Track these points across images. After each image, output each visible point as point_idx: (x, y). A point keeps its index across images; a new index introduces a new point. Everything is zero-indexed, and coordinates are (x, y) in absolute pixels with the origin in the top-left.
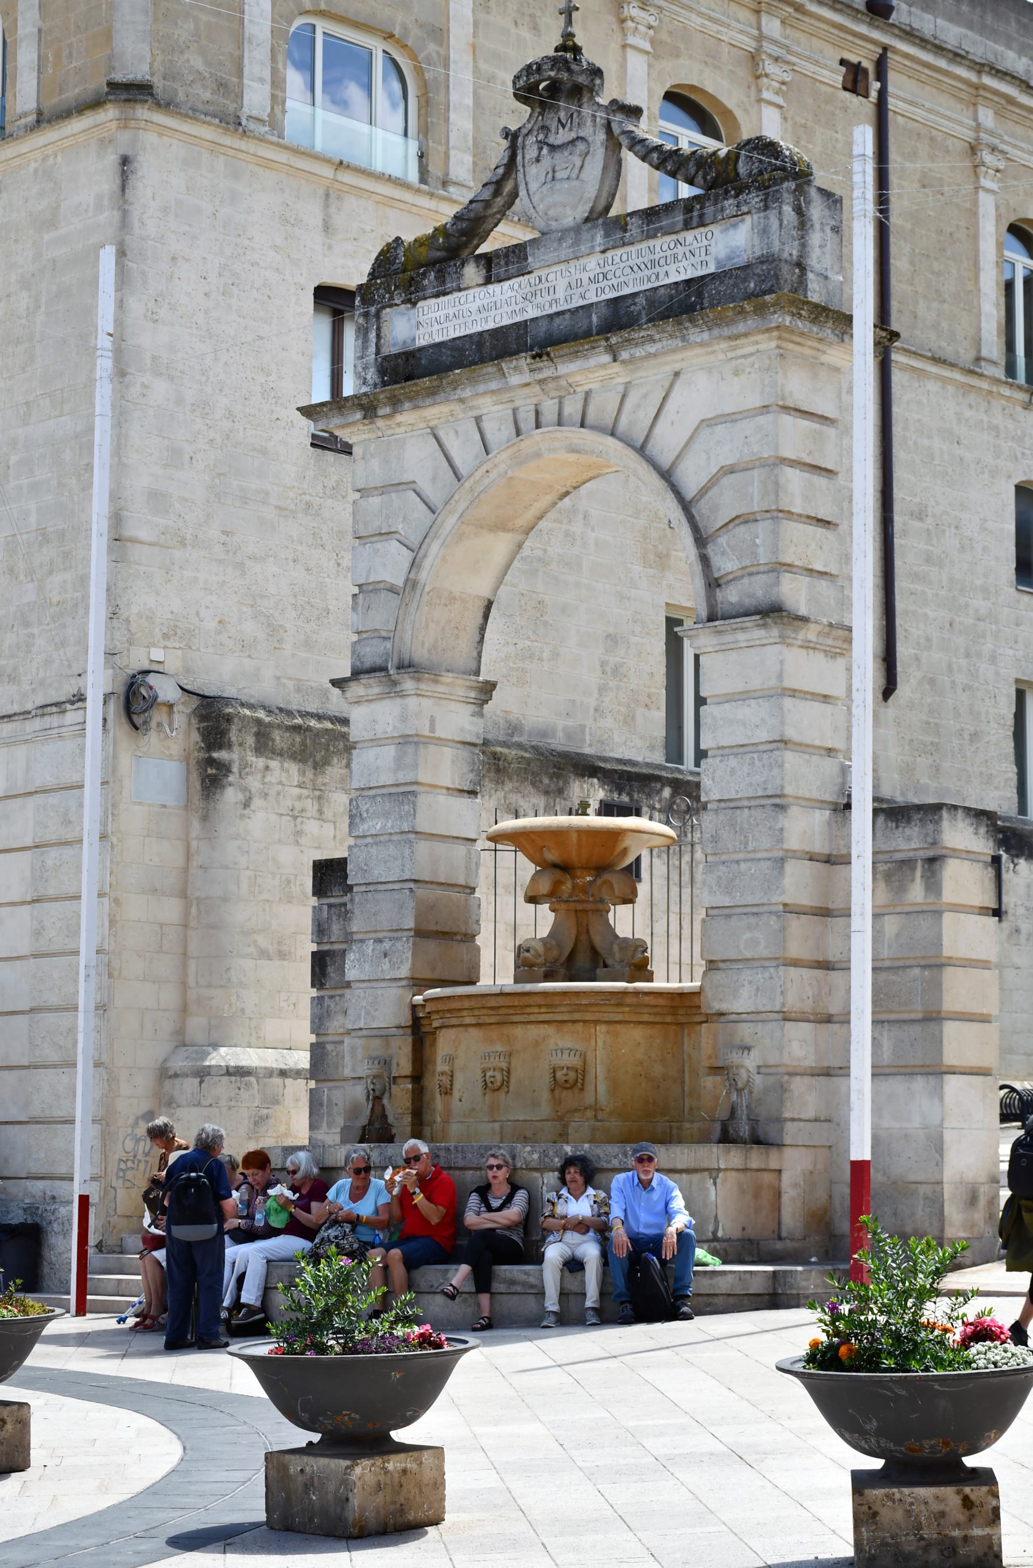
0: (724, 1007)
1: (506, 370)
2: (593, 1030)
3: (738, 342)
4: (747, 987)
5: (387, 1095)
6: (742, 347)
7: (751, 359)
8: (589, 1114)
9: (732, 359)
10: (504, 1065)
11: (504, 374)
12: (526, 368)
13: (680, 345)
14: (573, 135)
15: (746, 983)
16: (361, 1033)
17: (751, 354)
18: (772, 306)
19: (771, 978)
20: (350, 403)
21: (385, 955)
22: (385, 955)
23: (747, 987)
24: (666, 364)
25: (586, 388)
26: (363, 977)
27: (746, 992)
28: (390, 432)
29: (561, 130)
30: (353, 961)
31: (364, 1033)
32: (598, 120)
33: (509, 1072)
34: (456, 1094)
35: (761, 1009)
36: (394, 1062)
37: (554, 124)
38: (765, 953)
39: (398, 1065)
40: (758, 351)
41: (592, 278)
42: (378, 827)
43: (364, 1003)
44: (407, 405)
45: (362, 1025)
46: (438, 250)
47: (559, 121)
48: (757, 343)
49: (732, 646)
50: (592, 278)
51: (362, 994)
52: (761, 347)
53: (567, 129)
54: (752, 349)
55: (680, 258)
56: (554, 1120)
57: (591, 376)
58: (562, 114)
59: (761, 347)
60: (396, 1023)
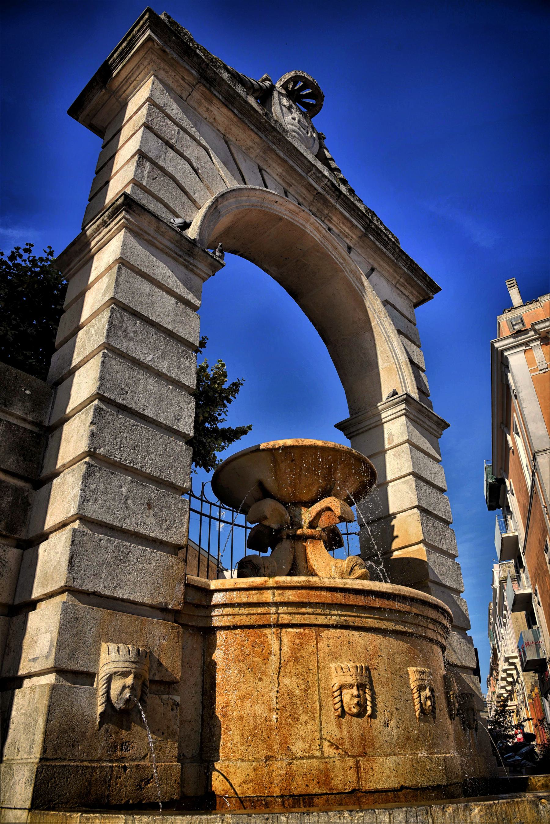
1: (312, 172)
3: (408, 286)
6: (406, 288)
9: (398, 288)
17: (405, 295)
20: (199, 61)
21: (149, 505)
22: (149, 505)
24: (375, 260)
25: (331, 226)
30: (94, 491)
42: (149, 358)
48: (412, 293)
49: (421, 422)
54: (406, 292)
57: (342, 225)
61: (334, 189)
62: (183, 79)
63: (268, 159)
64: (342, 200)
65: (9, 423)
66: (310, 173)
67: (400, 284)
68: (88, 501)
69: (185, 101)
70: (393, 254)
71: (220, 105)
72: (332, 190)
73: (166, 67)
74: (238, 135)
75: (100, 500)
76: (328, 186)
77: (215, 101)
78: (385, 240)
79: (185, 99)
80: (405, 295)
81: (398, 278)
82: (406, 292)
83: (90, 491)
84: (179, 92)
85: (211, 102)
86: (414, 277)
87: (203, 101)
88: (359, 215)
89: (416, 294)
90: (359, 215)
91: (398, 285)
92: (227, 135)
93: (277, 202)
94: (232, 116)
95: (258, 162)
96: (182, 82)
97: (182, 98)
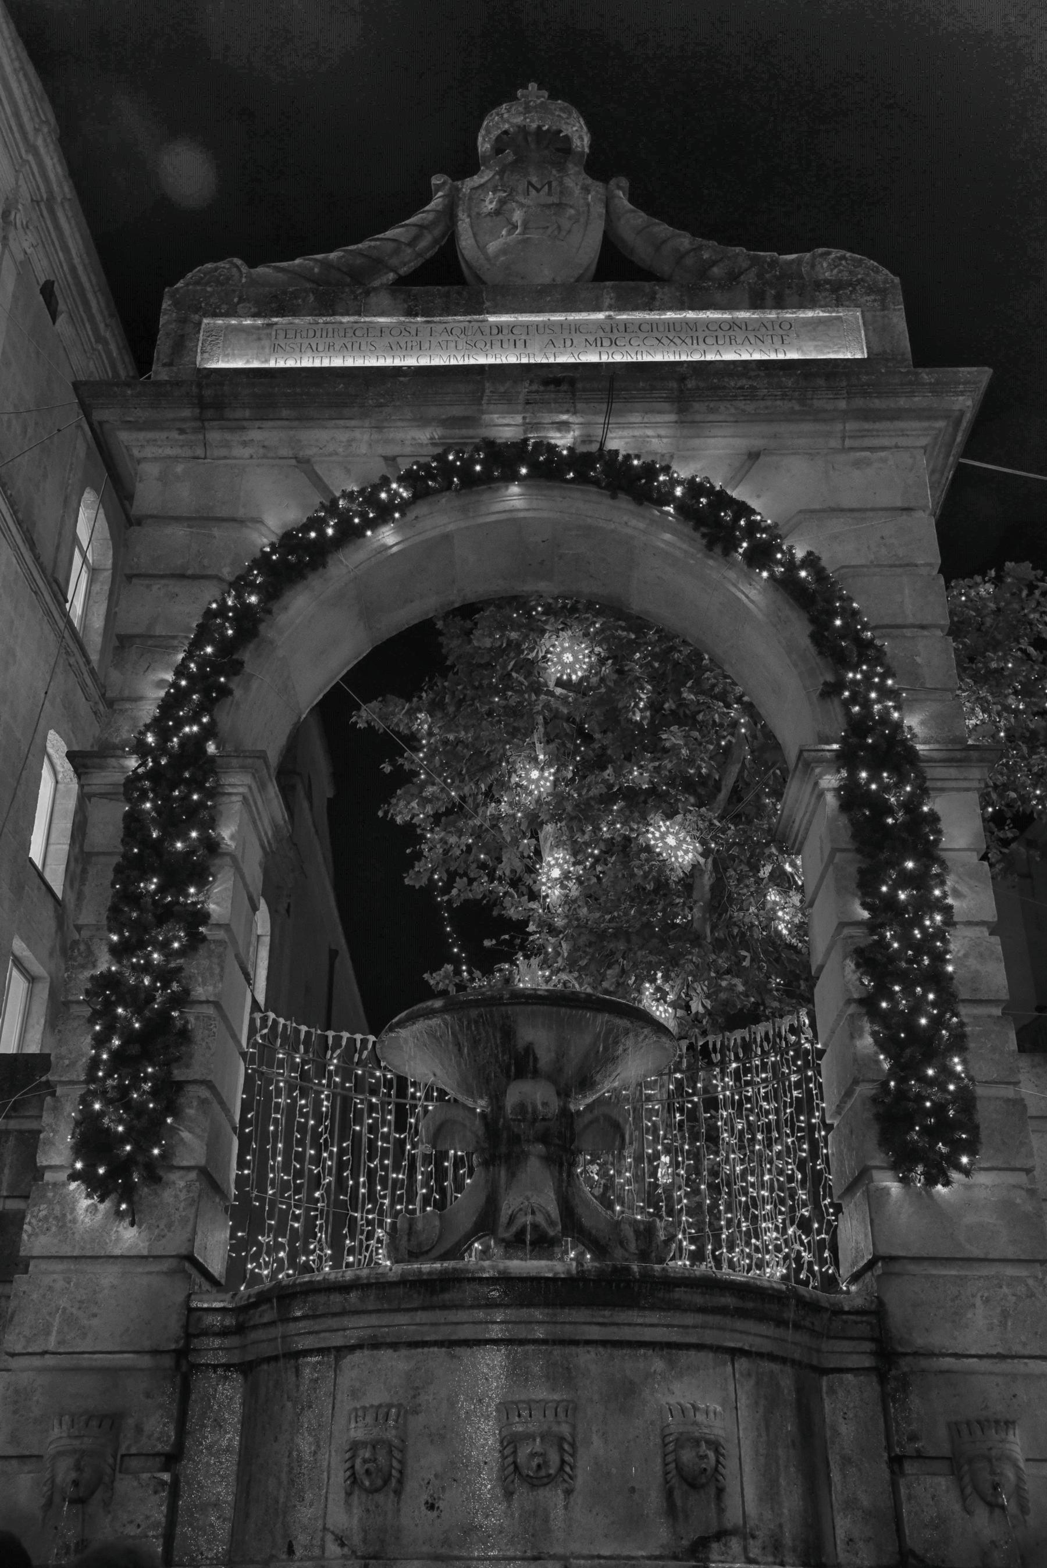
0: (938, 1340)
2: (729, 1368)
3: (877, 426)
4: (980, 1309)
5: (99, 1495)
7: (883, 454)
8: (735, 1545)
9: (852, 449)
10: (565, 1429)
11: (481, 398)
12: (522, 397)
13: (797, 407)
14: (555, 199)
15: (978, 1302)
16: (37, 1362)
17: (883, 448)
18: (965, 383)
19: (1031, 1295)
23: (980, 1309)
26: (66, 1250)
27: (979, 1317)
28: (223, 452)
29: (533, 192)
30: (46, 1218)
31: (50, 1361)
32: (593, 193)
33: (573, 1445)
34: (416, 1494)
35: (1017, 1349)
36: (131, 1421)
37: (522, 186)
38: (1010, 1252)
39: (139, 1429)
40: (897, 447)
41: (591, 339)
43: (63, 1302)
44: (285, 413)
45: (52, 1344)
46: (309, 280)
47: (530, 183)
48: (903, 434)
50: (591, 339)
51: (60, 1284)
52: (903, 441)
53: (541, 193)
54: (885, 442)
55: (739, 341)
56: (675, 1558)
58: (534, 180)
59: (903, 441)
60: (147, 1345)
61: (552, 387)
62: (182, 431)
63: (391, 436)
64: (584, 390)
65: (21, 1132)
66: (485, 398)
67: (850, 437)
68: (37, 1235)
69: (205, 458)
70: (784, 396)
71: (258, 424)
72: (550, 391)
73: (150, 435)
74: (317, 440)
75: (54, 1229)
76: (537, 392)
77: (245, 424)
78: (741, 388)
79: (203, 456)
80: (883, 448)
81: (839, 427)
82: (885, 442)
83: (40, 1220)
84: (188, 453)
85: (244, 428)
86: (877, 403)
87: (228, 436)
88: (643, 389)
89: (916, 424)
90: (643, 389)
91: (848, 443)
92: (301, 454)
93: (417, 517)
94: (286, 423)
95: (381, 450)
96: (182, 437)
97: (198, 458)
